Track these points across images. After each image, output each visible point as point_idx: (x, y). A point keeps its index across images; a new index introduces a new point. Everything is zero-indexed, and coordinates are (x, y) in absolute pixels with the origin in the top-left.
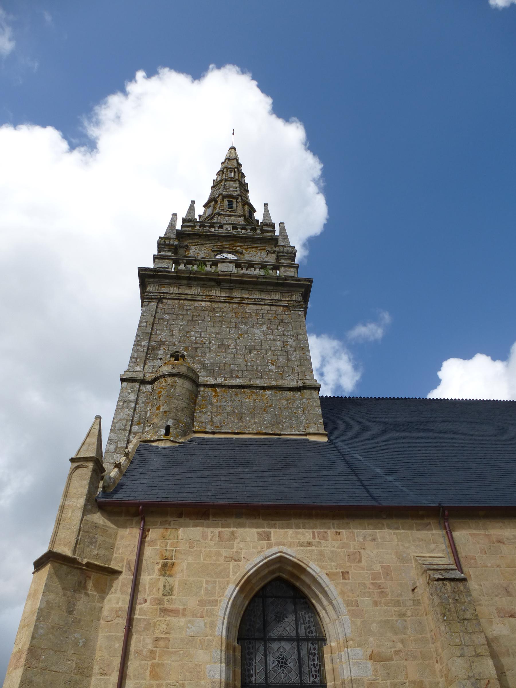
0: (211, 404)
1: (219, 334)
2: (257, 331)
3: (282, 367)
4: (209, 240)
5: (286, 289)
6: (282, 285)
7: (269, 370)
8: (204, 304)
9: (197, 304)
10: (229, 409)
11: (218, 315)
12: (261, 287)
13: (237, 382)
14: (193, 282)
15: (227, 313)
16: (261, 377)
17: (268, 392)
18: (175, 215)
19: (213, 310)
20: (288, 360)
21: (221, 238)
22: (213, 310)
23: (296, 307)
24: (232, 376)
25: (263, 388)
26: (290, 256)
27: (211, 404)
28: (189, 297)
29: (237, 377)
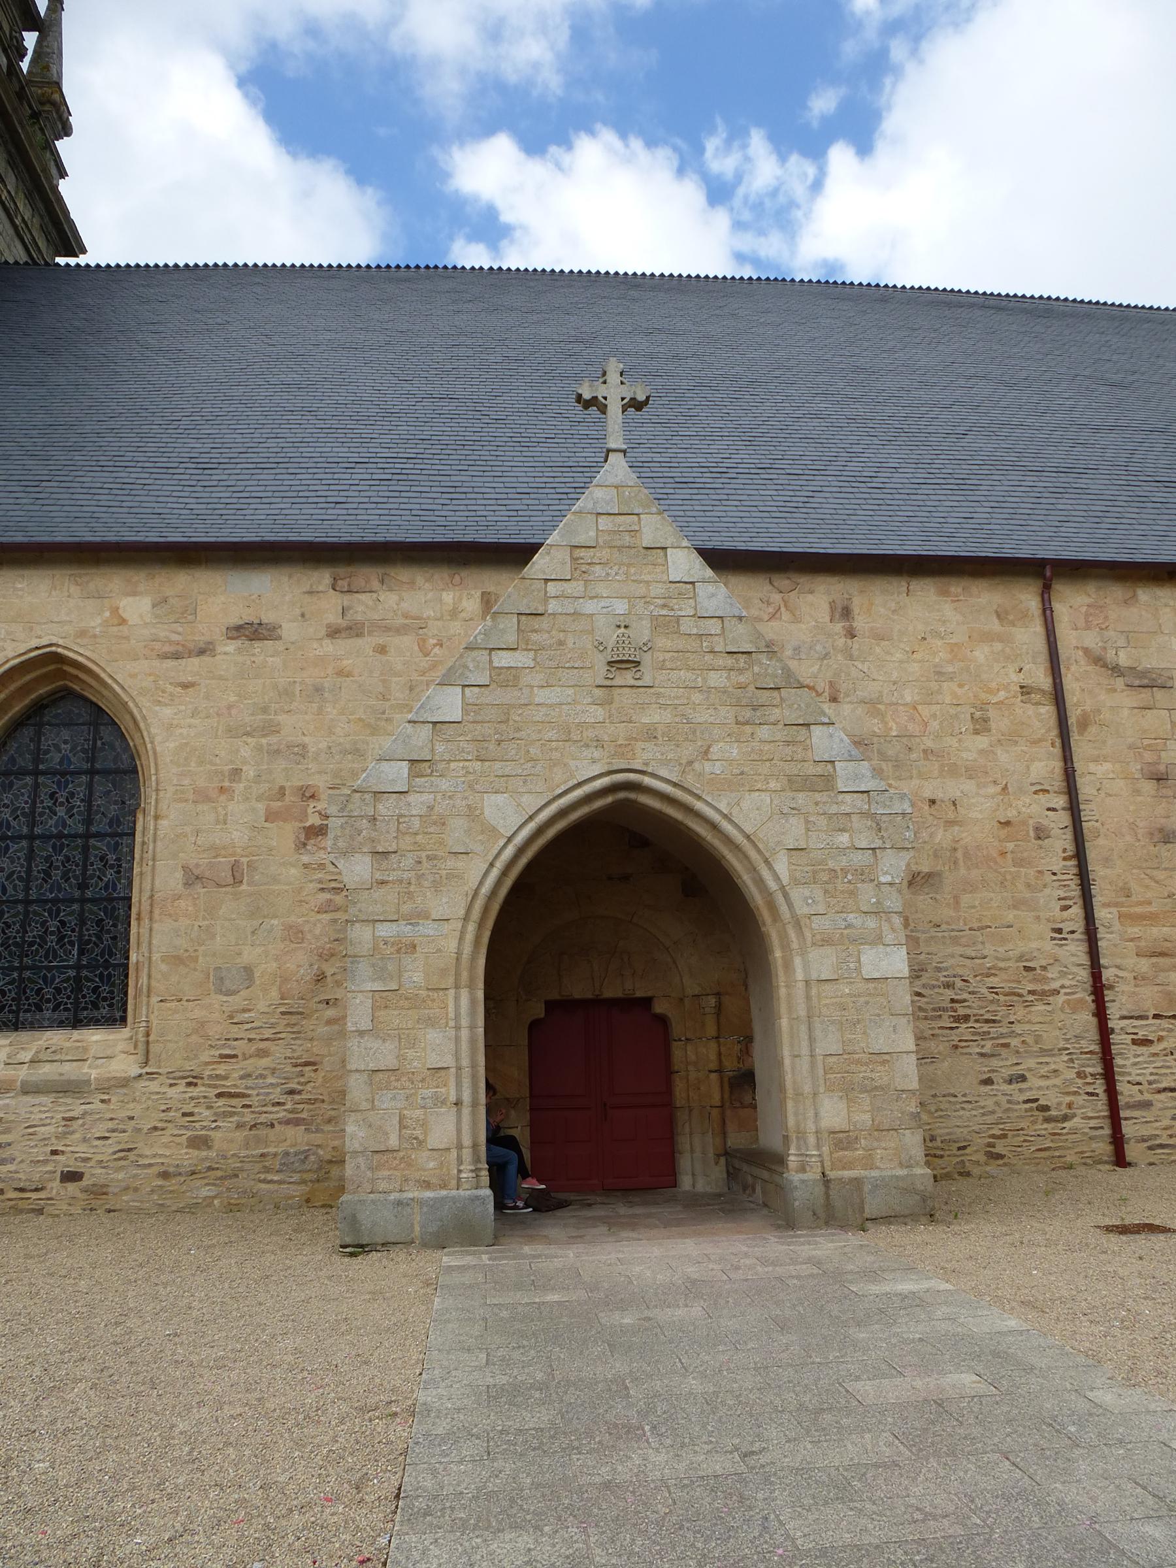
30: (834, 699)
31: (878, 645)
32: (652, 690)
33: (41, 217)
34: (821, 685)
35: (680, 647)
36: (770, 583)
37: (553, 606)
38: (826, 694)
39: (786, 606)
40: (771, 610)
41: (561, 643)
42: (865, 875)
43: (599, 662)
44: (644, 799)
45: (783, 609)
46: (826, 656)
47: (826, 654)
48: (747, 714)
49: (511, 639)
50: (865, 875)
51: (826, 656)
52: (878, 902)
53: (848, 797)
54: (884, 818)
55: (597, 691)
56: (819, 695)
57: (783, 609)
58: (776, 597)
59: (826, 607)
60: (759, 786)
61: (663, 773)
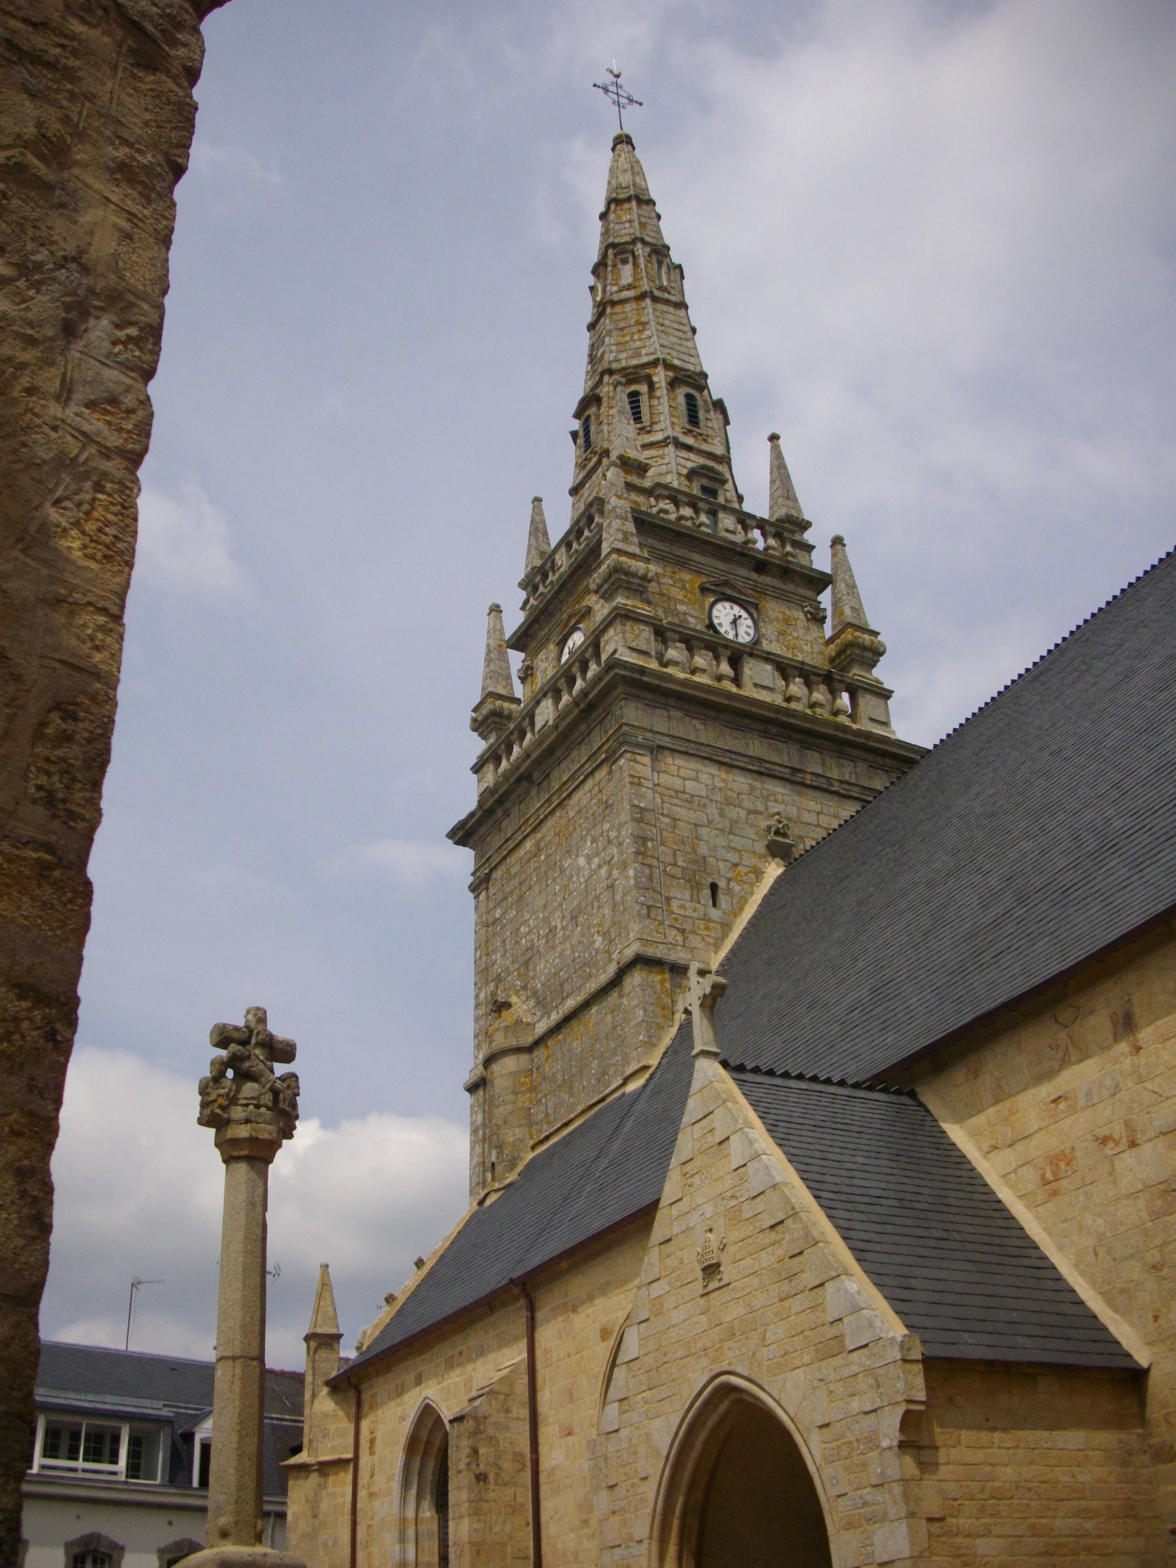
0: (544, 1079)
1: (545, 907)
2: (582, 861)
3: (609, 931)
4: (552, 615)
5: (600, 710)
6: (591, 707)
7: (597, 951)
8: (528, 844)
9: (521, 852)
10: (559, 1077)
11: (543, 857)
12: (573, 737)
13: (571, 1003)
14: (508, 805)
15: (550, 842)
16: (590, 976)
17: (594, 1009)
18: (496, 609)
19: (538, 850)
20: (614, 906)
21: (562, 596)
22: (538, 850)
23: (615, 752)
24: (563, 999)
25: (586, 1005)
26: (613, 584)
27: (544, 1079)
28: (511, 844)
29: (568, 997)
30: (1133, 1144)
31: (1164, 1049)
32: (730, 1287)
33: (865, 760)
34: (1118, 1130)
35: (743, 1235)
36: (1057, 1021)
37: (676, 1229)
38: (1124, 1140)
39: (1072, 1043)
40: (1060, 1055)
41: (681, 1261)
42: (871, 1441)
43: (698, 1268)
44: (745, 1397)
45: (1070, 1047)
46: (1116, 1090)
47: (1116, 1087)
48: (786, 1287)
49: (655, 1272)
50: (871, 1441)
51: (1116, 1090)
52: (883, 1472)
53: (855, 1354)
54: (881, 1371)
55: (702, 1301)
56: (1117, 1143)
57: (1070, 1047)
58: (1063, 1035)
59: (1107, 1023)
60: (797, 1363)
61: (739, 1370)
